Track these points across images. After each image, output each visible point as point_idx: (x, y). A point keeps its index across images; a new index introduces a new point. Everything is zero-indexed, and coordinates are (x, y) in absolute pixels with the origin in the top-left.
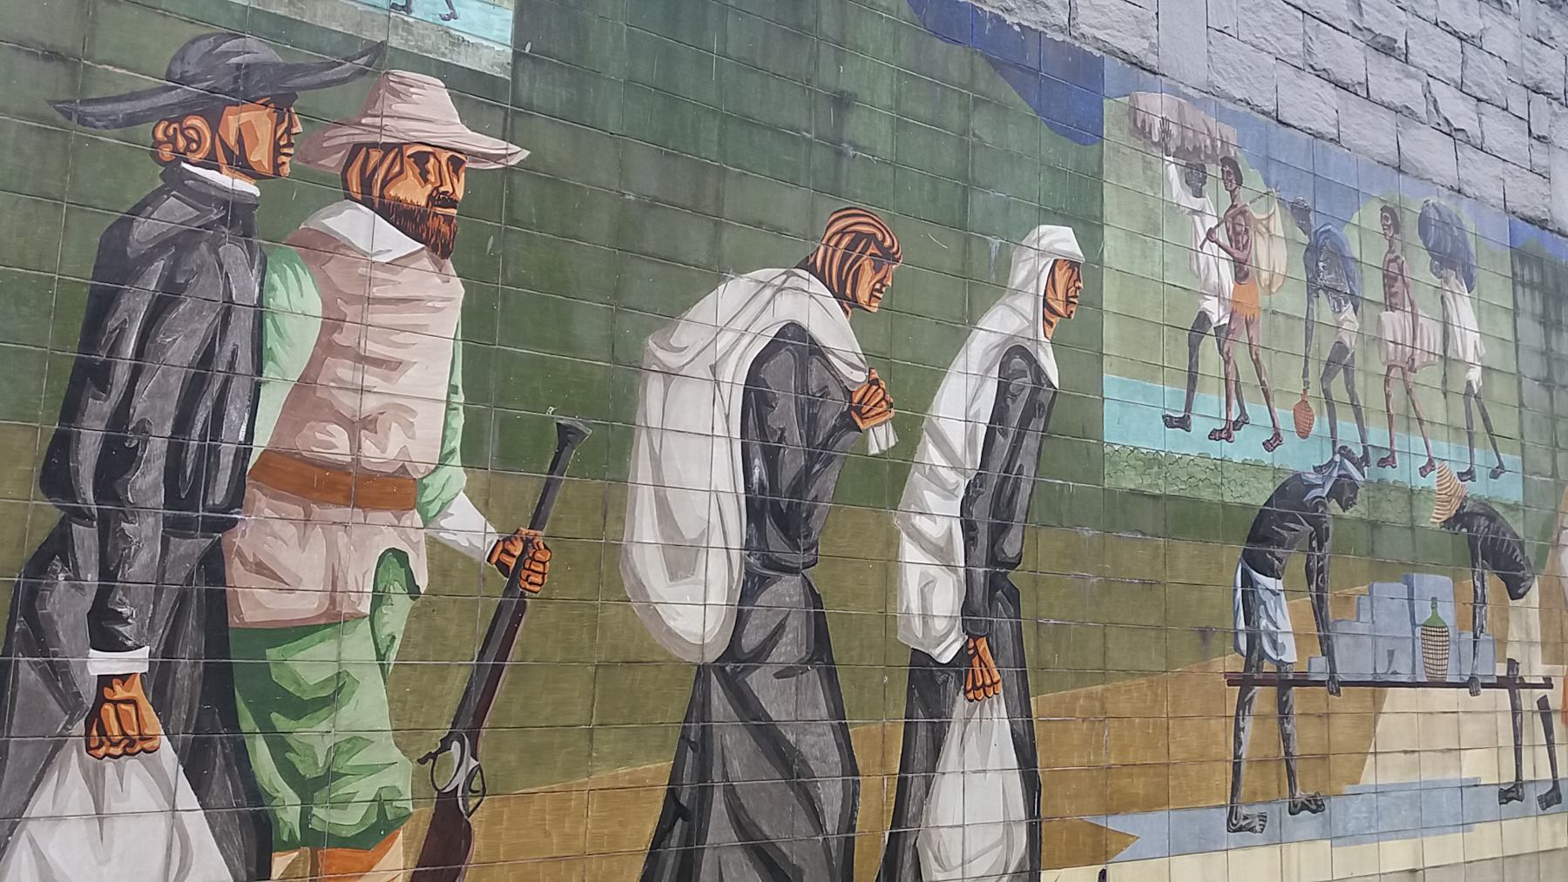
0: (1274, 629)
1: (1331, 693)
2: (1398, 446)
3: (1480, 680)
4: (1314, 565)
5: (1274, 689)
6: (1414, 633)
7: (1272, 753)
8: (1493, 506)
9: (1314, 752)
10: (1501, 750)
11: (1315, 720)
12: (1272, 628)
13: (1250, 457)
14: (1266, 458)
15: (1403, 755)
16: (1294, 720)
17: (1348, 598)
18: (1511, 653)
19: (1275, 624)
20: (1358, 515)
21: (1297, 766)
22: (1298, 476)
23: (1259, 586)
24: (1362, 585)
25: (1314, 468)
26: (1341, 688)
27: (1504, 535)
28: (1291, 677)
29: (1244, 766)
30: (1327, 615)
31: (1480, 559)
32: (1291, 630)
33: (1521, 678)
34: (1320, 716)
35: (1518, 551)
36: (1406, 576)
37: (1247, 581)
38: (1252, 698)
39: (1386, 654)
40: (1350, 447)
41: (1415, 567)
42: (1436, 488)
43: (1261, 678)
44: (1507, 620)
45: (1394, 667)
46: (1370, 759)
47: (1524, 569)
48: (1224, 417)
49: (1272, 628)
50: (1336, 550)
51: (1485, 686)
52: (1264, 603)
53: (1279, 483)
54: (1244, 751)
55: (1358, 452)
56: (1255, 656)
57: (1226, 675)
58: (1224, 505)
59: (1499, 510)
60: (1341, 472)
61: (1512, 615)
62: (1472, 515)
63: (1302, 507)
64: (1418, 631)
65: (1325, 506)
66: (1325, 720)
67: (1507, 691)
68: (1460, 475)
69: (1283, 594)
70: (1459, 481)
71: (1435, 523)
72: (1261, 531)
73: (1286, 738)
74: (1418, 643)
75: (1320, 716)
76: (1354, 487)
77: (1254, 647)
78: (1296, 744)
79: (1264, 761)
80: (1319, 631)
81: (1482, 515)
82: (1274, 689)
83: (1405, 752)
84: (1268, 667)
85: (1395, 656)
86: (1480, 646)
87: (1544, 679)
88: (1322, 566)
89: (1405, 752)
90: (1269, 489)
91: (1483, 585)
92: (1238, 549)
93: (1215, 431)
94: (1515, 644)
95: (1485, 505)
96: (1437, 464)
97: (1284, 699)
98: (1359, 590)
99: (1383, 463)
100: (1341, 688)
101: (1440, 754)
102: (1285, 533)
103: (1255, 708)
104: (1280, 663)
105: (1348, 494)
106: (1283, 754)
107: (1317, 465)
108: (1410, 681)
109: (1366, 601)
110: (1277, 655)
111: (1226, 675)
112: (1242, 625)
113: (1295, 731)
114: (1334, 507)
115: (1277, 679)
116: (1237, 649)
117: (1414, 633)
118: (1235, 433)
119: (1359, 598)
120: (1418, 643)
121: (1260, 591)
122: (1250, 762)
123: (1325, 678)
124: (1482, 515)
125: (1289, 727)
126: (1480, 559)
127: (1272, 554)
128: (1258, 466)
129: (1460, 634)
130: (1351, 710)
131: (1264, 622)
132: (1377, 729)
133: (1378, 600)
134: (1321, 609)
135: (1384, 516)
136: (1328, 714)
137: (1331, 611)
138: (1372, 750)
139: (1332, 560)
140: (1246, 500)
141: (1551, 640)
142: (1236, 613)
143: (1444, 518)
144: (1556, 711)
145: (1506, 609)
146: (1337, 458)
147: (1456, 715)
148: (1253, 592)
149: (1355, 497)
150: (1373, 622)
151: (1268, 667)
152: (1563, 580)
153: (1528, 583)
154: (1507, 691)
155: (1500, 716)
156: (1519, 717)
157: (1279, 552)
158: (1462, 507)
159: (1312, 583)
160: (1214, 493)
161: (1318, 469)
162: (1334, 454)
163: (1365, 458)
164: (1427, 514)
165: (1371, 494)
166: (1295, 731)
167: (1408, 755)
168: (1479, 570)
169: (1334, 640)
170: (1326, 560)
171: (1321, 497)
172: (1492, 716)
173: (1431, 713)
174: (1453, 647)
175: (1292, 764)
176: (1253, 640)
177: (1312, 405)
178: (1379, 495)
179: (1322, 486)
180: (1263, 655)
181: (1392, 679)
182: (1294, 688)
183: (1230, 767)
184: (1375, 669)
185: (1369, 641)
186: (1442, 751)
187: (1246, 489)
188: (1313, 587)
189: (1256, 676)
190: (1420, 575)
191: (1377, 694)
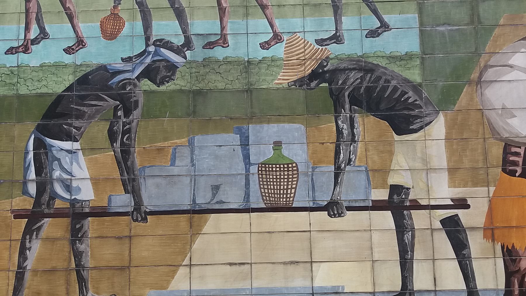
0: (69, 177)
1: (136, 220)
2: (231, 29)
3: (345, 204)
4: (119, 127)
5: (65, 221)
6: (247, 170)
7: (61, 264)
8: (370, 60)
9: (110, 265)
10: (376, 264)
11: (113, 241)
12: (65, 176)
13: (50, 60)
14: (68, 59)
15: (228, 267)
16: (87, 241)
17: (160, 150)
18: (394, 180)
19: (70, 174)
20: (178, 87)
21: (90, 276)
22: (103, 68)
23: (52, 149)
24: (184, 138)
25: (122, 59)
26: (148, 217)
27: (388, 81)
28: (87, 210)
29: (28, 276)
30: (133, 162)
31: (347, 106)
32: (89, 177)
33: (415, 201)
34: (120, 238)
35: (411, 93)
36: (237, 128)
37: (39, 145)
38: (42, 226)
39: (209, 189)
40: (167, 39)
41: (252, 118)
42: (282, 56)
43: (52, 212)
44: (391, 153)
45: (221, 196)
46: (182, 271)
47: (421, 107)
48: (22, 37)
49: (65, 176)
50: (146, 115)
51: (349, 209)
52: (59, 160)
53: (79, 75)
54: (29, 264)
55: (179, 41)
56: (46, 197)
57: (13, 211)
58: (19, 97)
59: (383, 63)
60: (155, 58)
61: (398, 149)
62: (336, 71)
63: (106, 88)
64: (254, 169)
65: (135, 85)
66: (127, 241)
67: (390, 211)
68: (320, 42)
69: (80, 153)
70: (321, 48)
71: (281, 84)
72: (59, 110)
73: (78, 255)
74: (254, 180)
75: (120, 238)
76: (172, 67)
77: (44, 190)
78: (89, 258)
79: (53, 271)
80: (122, 174)
81: (354, 69)
82: (65, 221)
83: (231, 264)
84: (58, 204)
85: (221, 189)
86: (345, 178)
87: (452, 200)
88: (130, 129)
89: (231, 264)
90: (69, 79)
91: (352, 126)
92: (31, 126)
93: (12, 48)
94: (403, 173)
95: (359, 61)
96: (285, 37)
97: (78, 226)
98: (176, 143)
99: (210, 45)
100: (148, 217)
101: (282, 265)
102: (85, 109)
103: (43, 233)
104: (73, 202)
105: (163, 73)
106: (74, 265)
107: (124, 57)
108: (241, 207)
109: (186, 151)
110: (71, 195)
111: (13, 211)
112: (32, 175)
113: (89, 249)
114: (146, 84)
115: (71, 212)
116: (25, 192)
117: (247, 170)
118: (34, 47)
119: (175, 149)
120: (254, 180)
121: (55, 152)
122: (35, 272)
123: (130, 209)
124: (354, 69)
125: (82, 247)
126: (347, 106)
127: (70, 125)
128: (58, 66)
129: (314, 169)
130: (161, 233)
131: (57, 173)
132: (195, 247)
133: (201, 148)
134: (125, 160)
135: (211, 86)
136: (130, 237)
137: (138, 161)
138: (186, 262)
139: (142, 123)
140: (44, 90)
141: (467, 163)
142: (26, 169)
143: (295, 78)
144: (473, 229)
145: (391, 144)
146: (152, 49)
147: (308, 233)
148: (46, 154)
149: (174, 74)
150: (193, 165)
151: (58, 204)
152: (486, 112)
153: (428, 119)
154: (390, 211)
155: (376, 237)
156: (408, 237)
157: (77, 123)
158: (321, 66)
159: (116, 141)
160: (9, 89)
161: (128, 60)
162: (147, 45)
163: (188, 44)
164: (269, 78)
165: (194, 70)
166: (89, 249)
167: (234, 267)
168: (345, 114)
169: (142, 181)
170: (134, 124)
171: (130, 79)
172: (367, 235)
173: (269, 232)
174: (302, 178)
175: (85, 274)
176: (41, 188)
177: (123, 15)
178: (202, 71)
179: (133, 71)
180: (54, 196)
181: (217, 207)
182: (89, 218)
183: (12, 276)
184: (194, 201)
185: (187, 180)
186: (285, 263)
187: (44, 83)
188: (117, 145)
189: (46, 211)
190: (258, 127)
191: (195, 220)
